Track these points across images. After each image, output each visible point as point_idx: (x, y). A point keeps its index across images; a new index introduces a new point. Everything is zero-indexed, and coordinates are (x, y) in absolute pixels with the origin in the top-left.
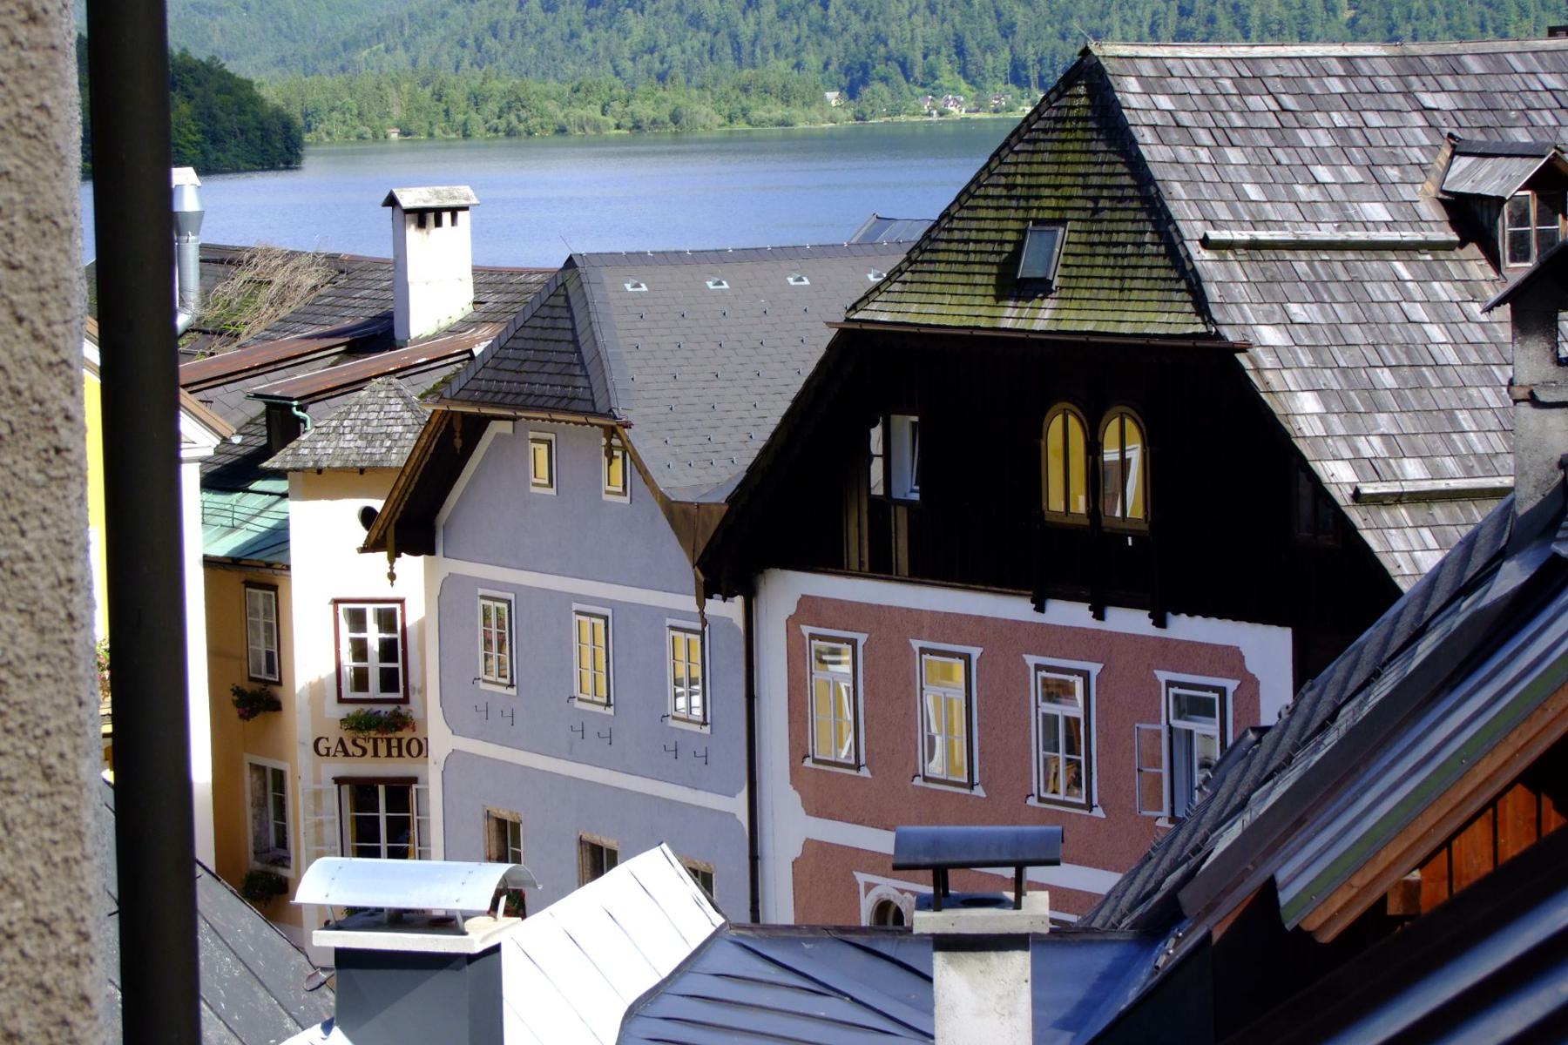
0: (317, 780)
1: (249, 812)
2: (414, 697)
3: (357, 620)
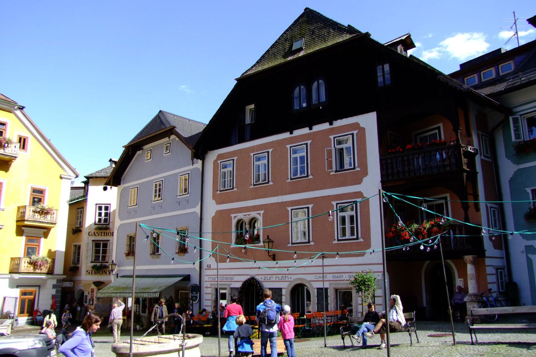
0: (88, 240)
1: (72, 255)
2: (111, 224)
3: (100, 208)
